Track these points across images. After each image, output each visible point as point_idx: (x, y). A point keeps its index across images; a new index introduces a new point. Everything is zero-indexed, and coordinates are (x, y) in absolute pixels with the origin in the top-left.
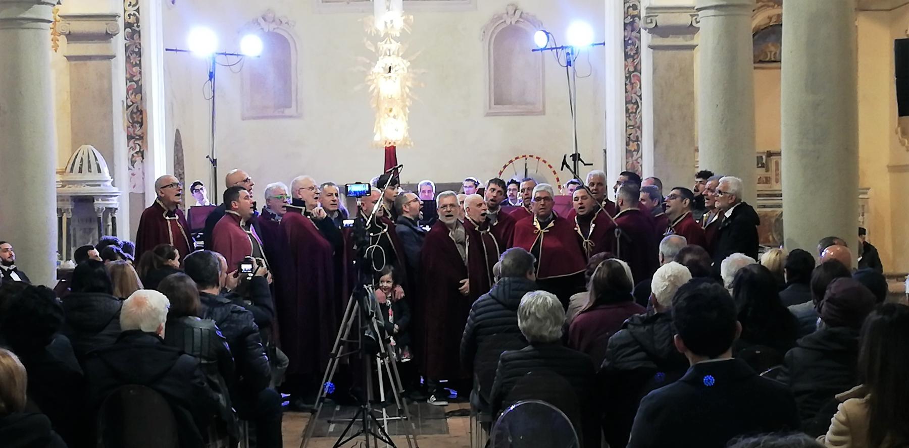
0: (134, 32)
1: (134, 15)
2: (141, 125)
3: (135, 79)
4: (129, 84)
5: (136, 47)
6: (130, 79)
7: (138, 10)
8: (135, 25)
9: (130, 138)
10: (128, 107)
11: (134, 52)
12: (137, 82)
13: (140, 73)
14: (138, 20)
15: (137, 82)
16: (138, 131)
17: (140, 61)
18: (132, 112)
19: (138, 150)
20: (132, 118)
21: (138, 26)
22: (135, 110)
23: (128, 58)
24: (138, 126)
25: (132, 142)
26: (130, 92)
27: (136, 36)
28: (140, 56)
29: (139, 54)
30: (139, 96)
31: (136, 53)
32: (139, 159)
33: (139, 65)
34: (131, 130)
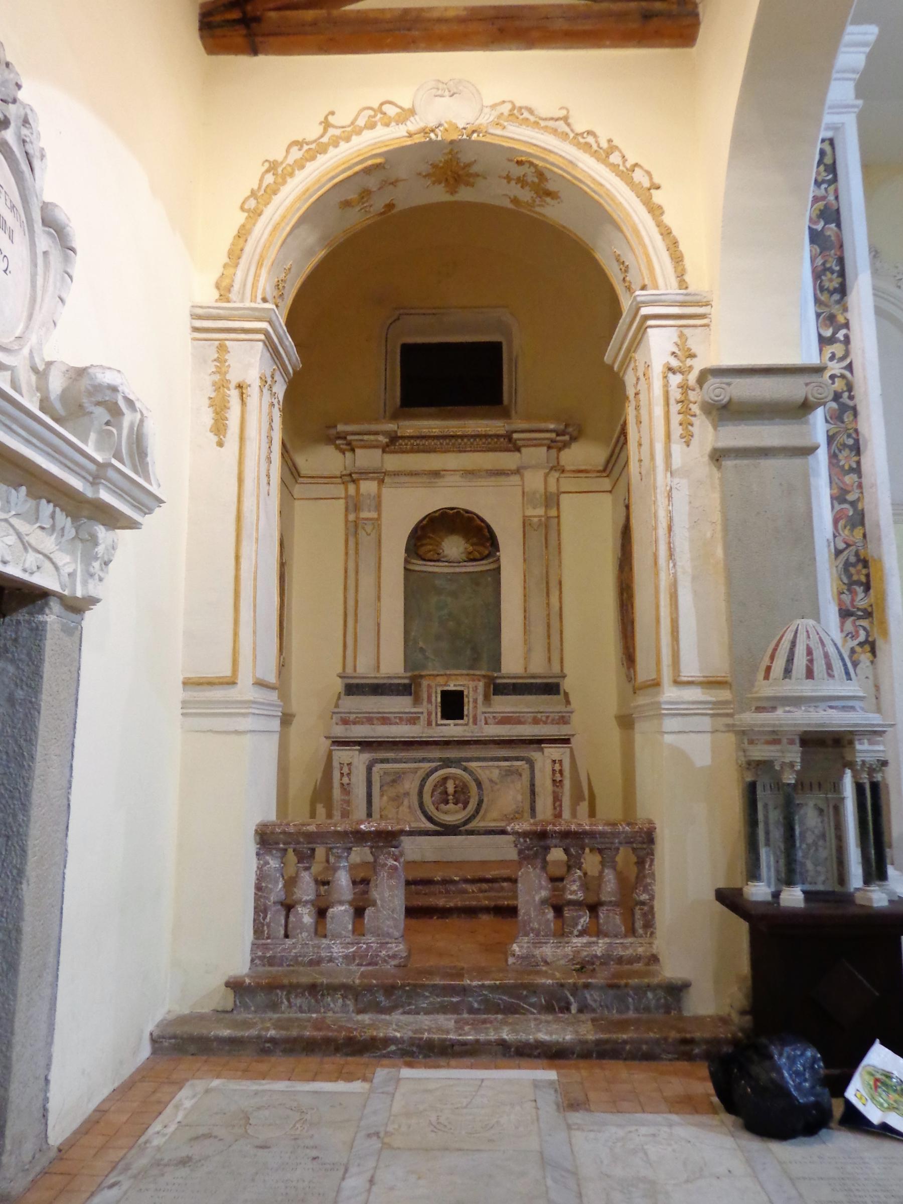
0: (844, 408)
1: (843, 376)
2: (867, 587)
3: (851, 497)
4: (838, 507)
5: (849, 436)
6: (839, 497)
7: (850, 367)
8: (846, 395)
9: (845, 614)
10: (838, 553)
11: (844, 446)
12: (853, 504)
13: (860, 486)
14: (850, 387)
15: (853, 504)
16: (861, 600)
17: (858, 463)
18: (847, 565)
19: (862, 636)
20: (850, 576)
21: (851, 398)
22: (853, 559)
23: (833, 457)
24: (860, 590)
25: (849, 622)
26: (841, 523)
27: (848, 417)
28: (858, 452)
29: (857, 449)
30: (858, 532)
31: (851, 448)
32: (865, 658)
33: (857, 470)
34: (847, 598)
